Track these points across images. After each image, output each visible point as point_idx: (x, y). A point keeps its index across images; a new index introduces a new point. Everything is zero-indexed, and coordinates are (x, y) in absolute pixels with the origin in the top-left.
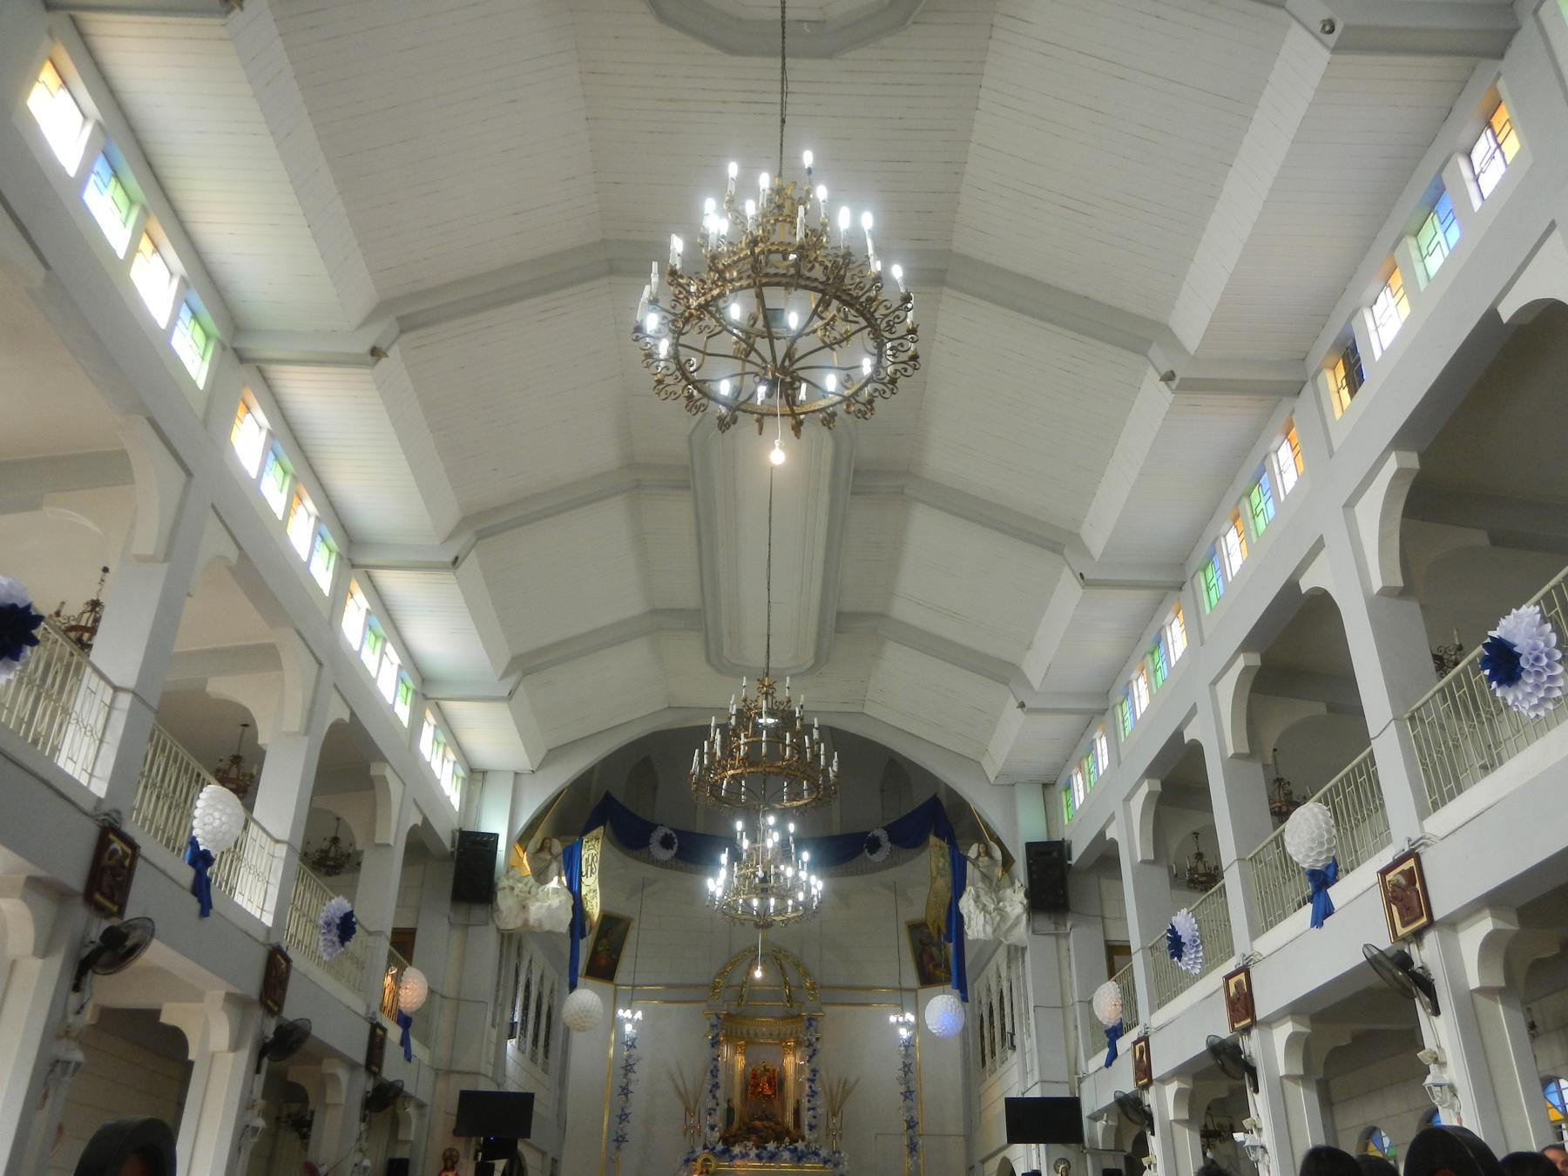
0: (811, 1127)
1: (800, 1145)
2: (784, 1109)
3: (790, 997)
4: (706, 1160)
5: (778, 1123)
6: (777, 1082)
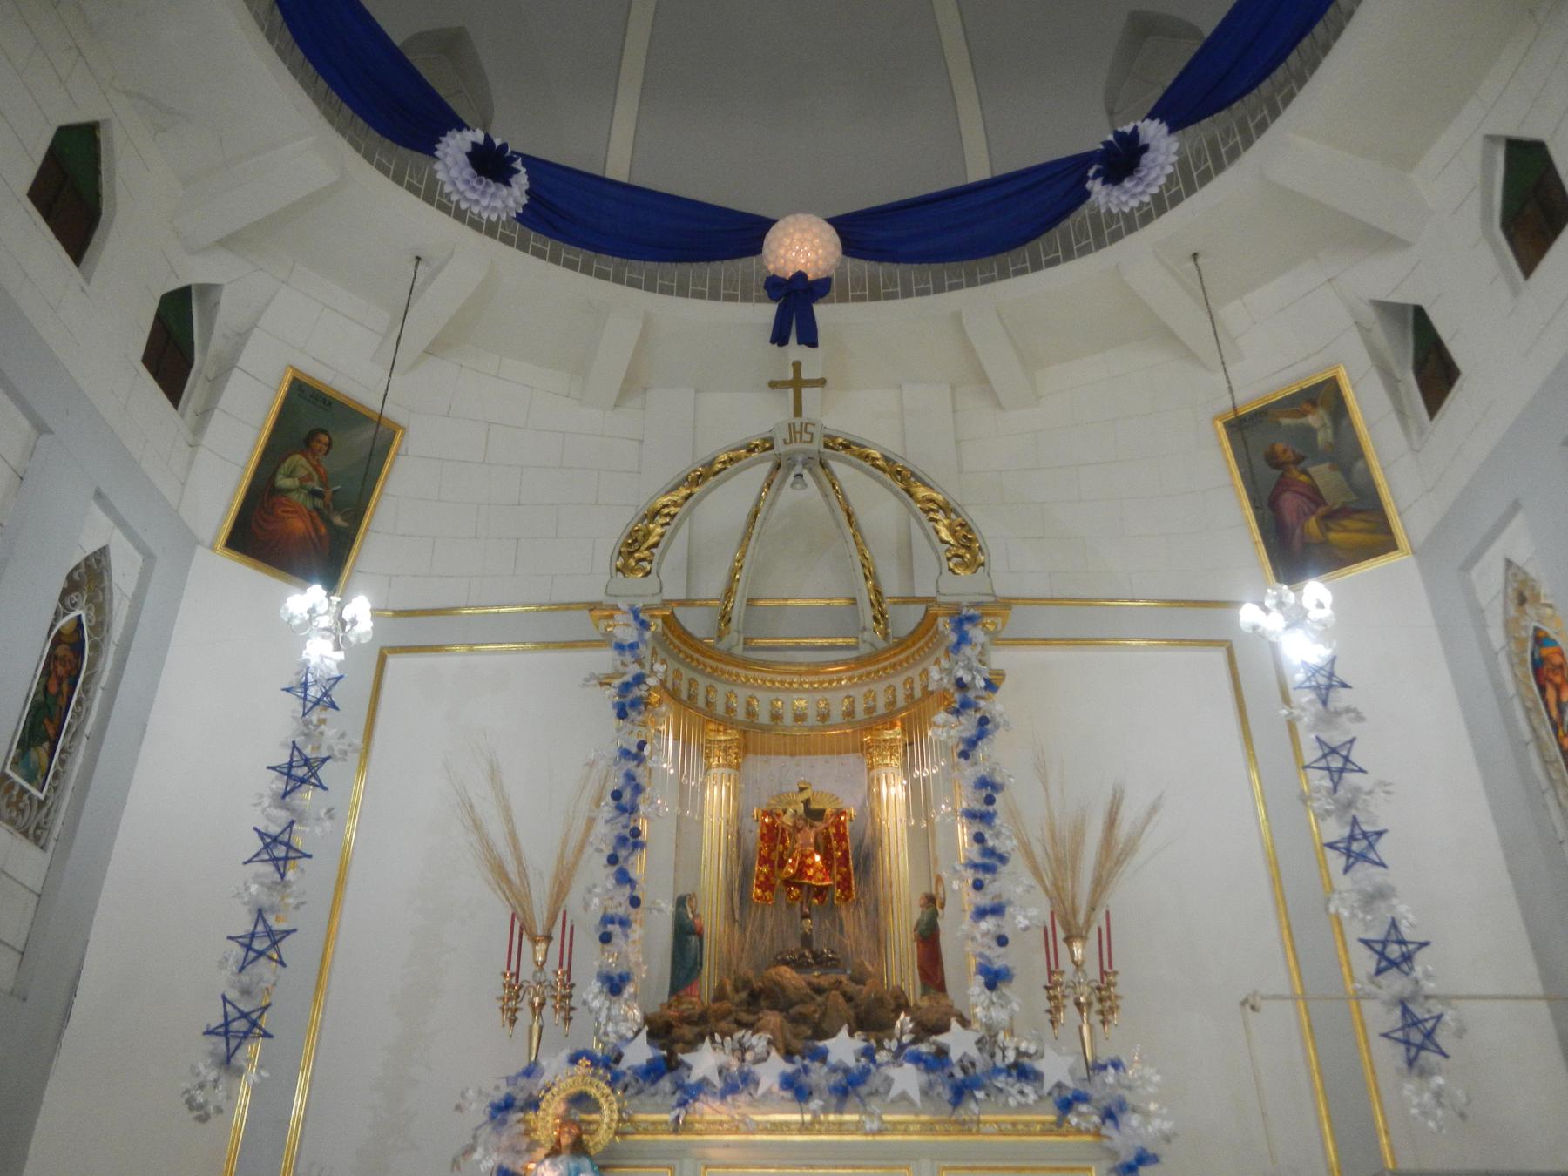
0: (994, 978)
1: (959, 1042)
2: (878, 937)
3: (880, 617)
4: (580, 1100)
5: (858, 980)
6: (850, 858)
